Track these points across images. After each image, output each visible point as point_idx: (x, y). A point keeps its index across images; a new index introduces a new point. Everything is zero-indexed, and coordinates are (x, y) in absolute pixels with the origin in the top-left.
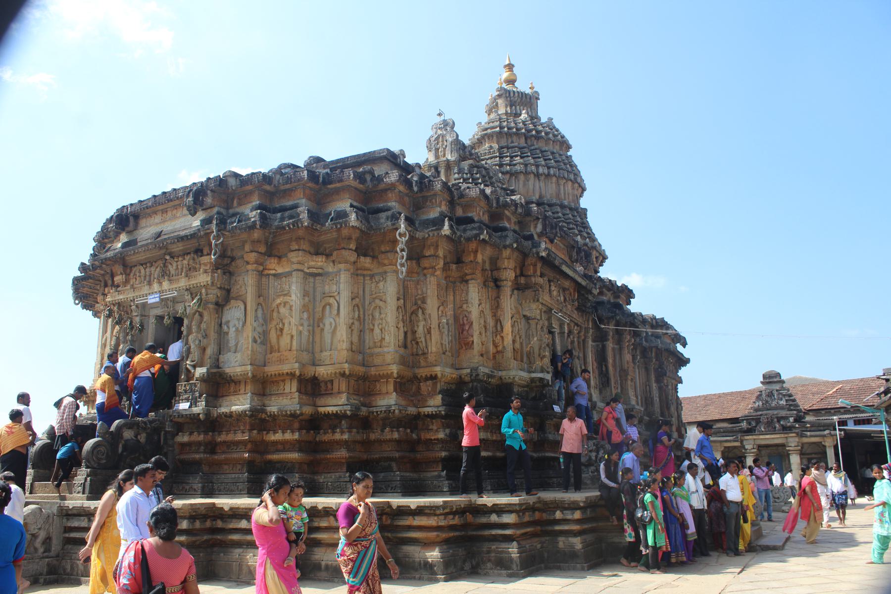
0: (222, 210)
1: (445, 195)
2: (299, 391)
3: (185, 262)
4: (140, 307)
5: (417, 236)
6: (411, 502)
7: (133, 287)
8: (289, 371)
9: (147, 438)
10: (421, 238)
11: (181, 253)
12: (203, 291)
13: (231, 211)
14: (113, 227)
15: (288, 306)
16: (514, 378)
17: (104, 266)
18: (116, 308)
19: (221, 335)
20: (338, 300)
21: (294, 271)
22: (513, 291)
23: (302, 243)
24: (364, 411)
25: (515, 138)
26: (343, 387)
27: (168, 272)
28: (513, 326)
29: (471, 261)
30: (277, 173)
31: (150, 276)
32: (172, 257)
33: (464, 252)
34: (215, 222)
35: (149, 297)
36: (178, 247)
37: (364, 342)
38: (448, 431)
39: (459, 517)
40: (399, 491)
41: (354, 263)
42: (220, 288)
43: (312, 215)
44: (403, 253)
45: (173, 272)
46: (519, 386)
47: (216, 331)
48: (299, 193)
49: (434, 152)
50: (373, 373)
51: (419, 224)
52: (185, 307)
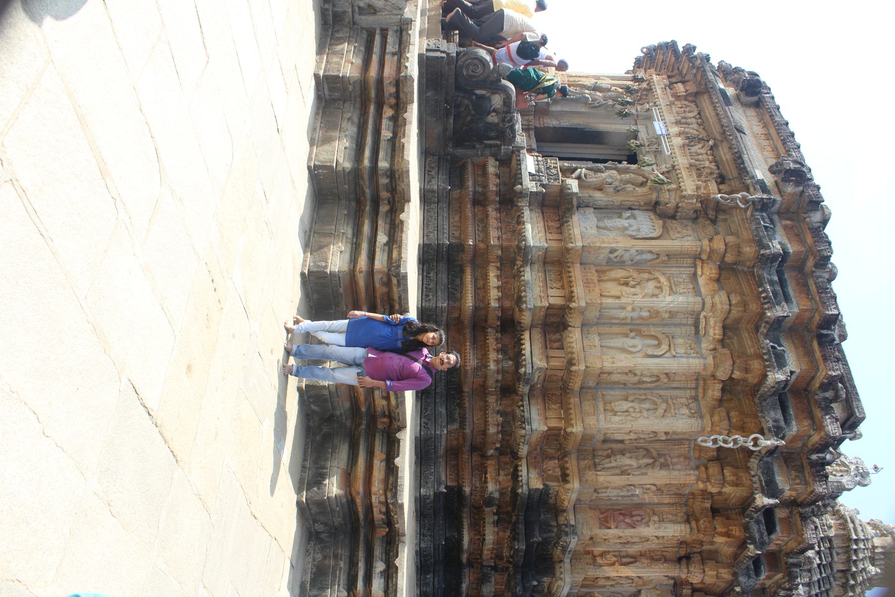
0: (777, 206)
1: (805, 496)
2: (551, 307)
3: (707, 164)
4: (648, 113)
5: (752, 460)
6: (404, 458)
7: (671, 104)
8: (575, 294)
9: (492, 124)
10: (749, 464)
11: (718, 158)
12: (674, 186)
13: (776, 217)
14: (745, 76)
15: (657, 291)
16: (561, 579)
17: (694, 71)
18: (644, 85)
19: (618, 210)
20: (665, 356)
21: (703, 299)
22: (673, 578)
23: (740, 309)
24: (524, 389)
25: (843, 557)
26: (554, 363)
27: (693, 143)
28: (627, 577)
29: (715, 528)
30: (830, 275)
31: (686, 123)
32: (711, 148)
33: (727, 519)
34: (765, 196)
35: (661, 123)
36: (725, 155)
37: (611, 389)
38: (496, 495)
39: (382, 519)
40: (422, 433)
41: (713, 376)
42: (677, 207)
43: (779, 321)
44: (732, 444)
45: (693, 149)
46: (551, 583)
47: (624, 203)
48: (806, 304)
50: (572, 400)
51: (768, 462)
52: (651, 165)
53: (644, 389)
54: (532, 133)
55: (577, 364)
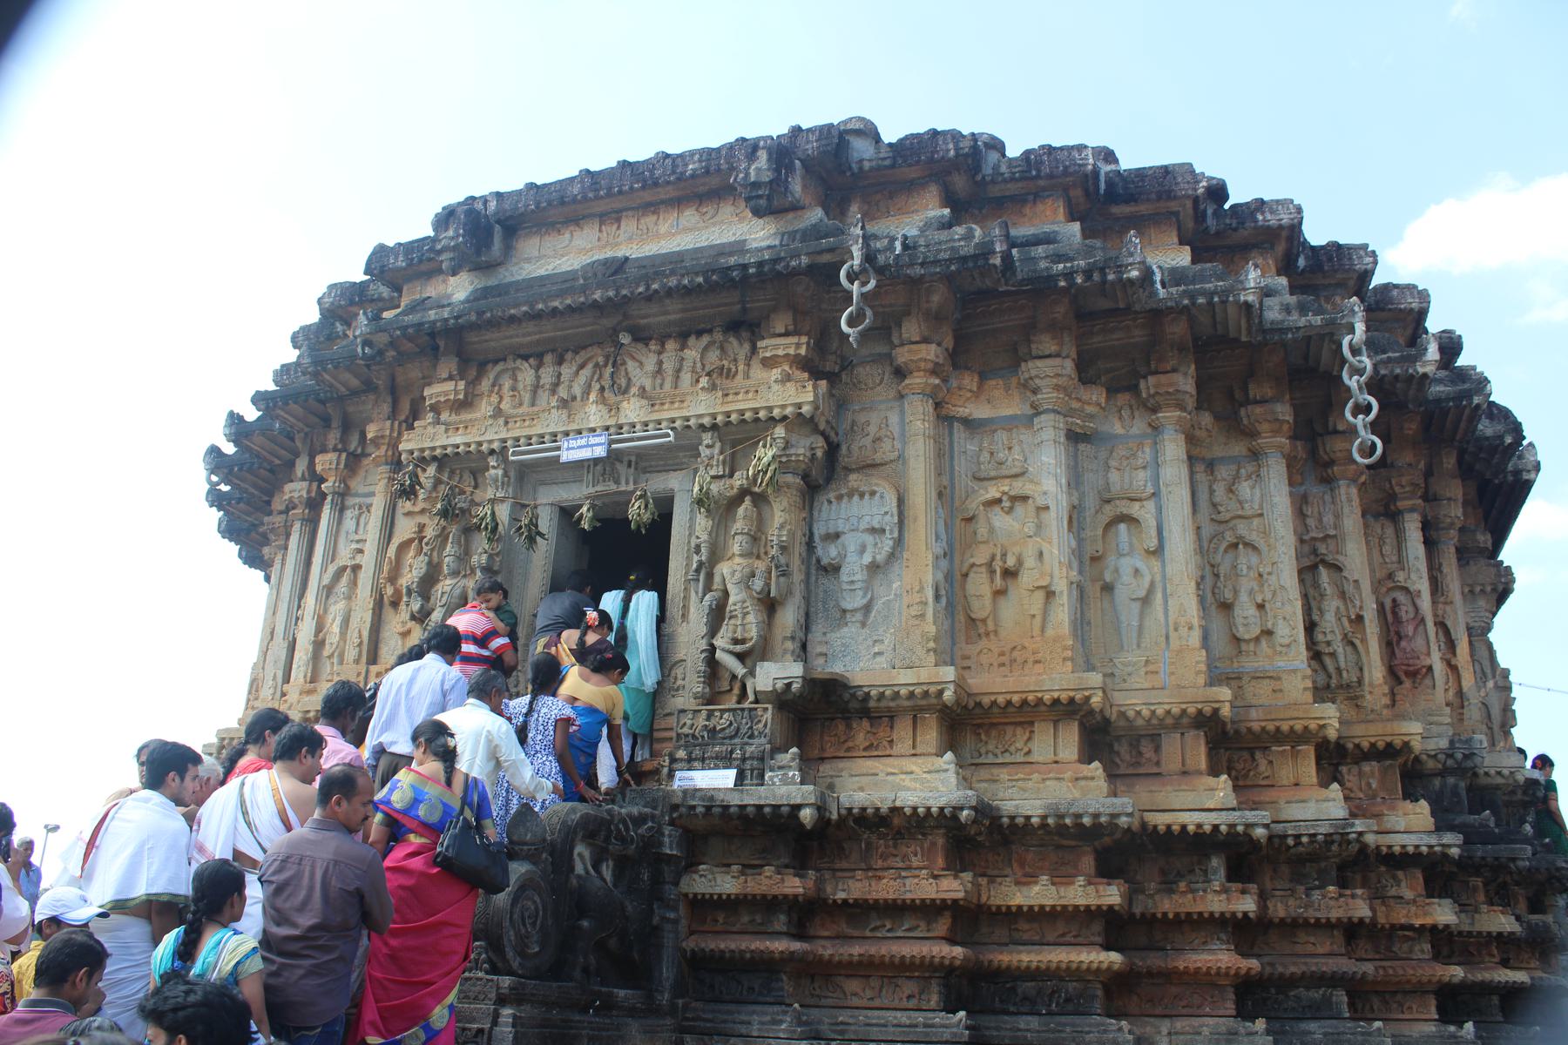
3: (691, 354)
8: (1064, 696)
29: (1410, 465)
36: (666, 313)
55: (1216, 705)
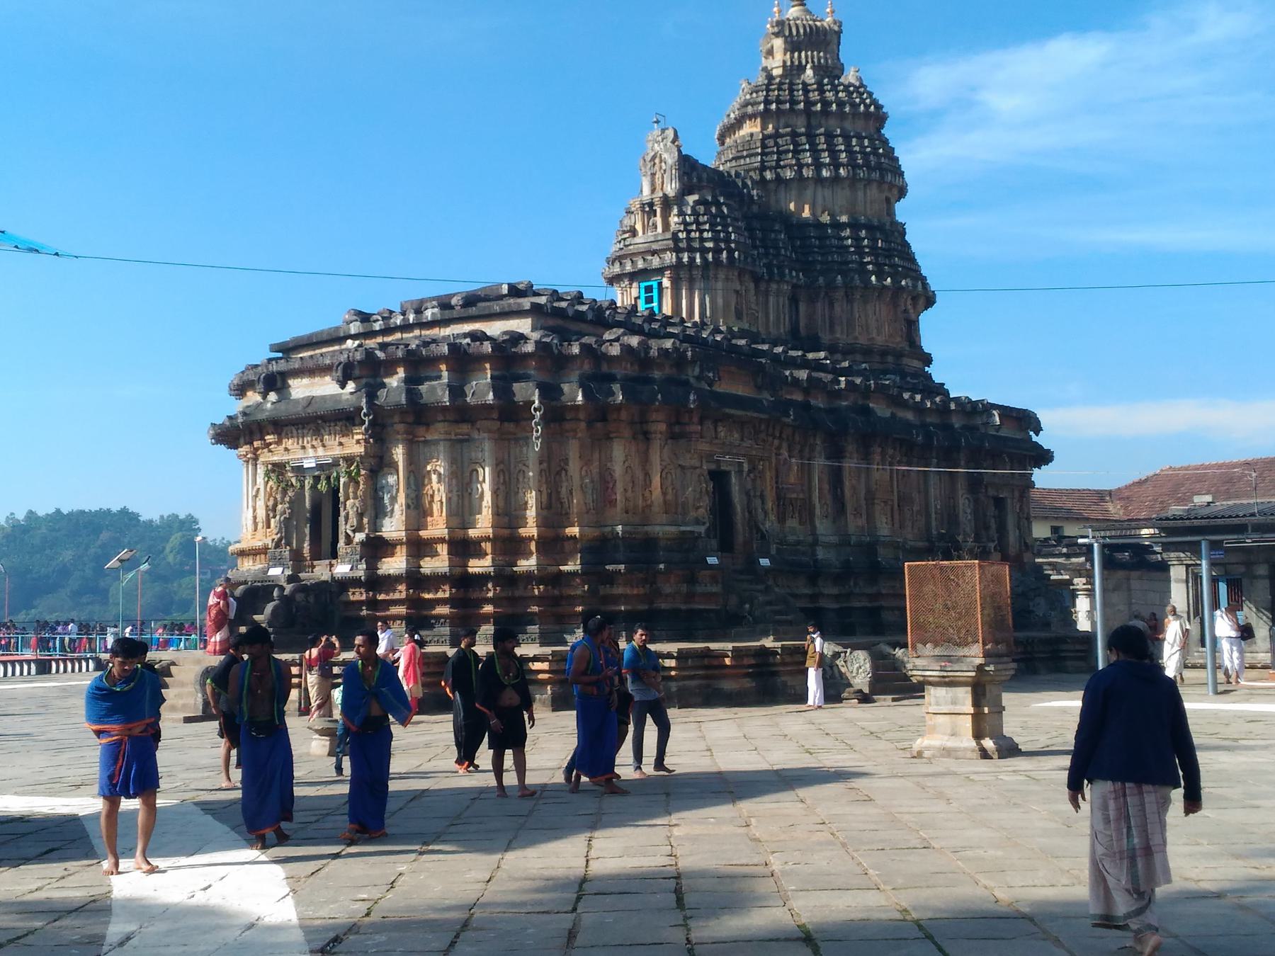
37: (510, 504)
42: (374, 457)
49: (649, 178)
53: (510, 479)
54: (315, 563)
